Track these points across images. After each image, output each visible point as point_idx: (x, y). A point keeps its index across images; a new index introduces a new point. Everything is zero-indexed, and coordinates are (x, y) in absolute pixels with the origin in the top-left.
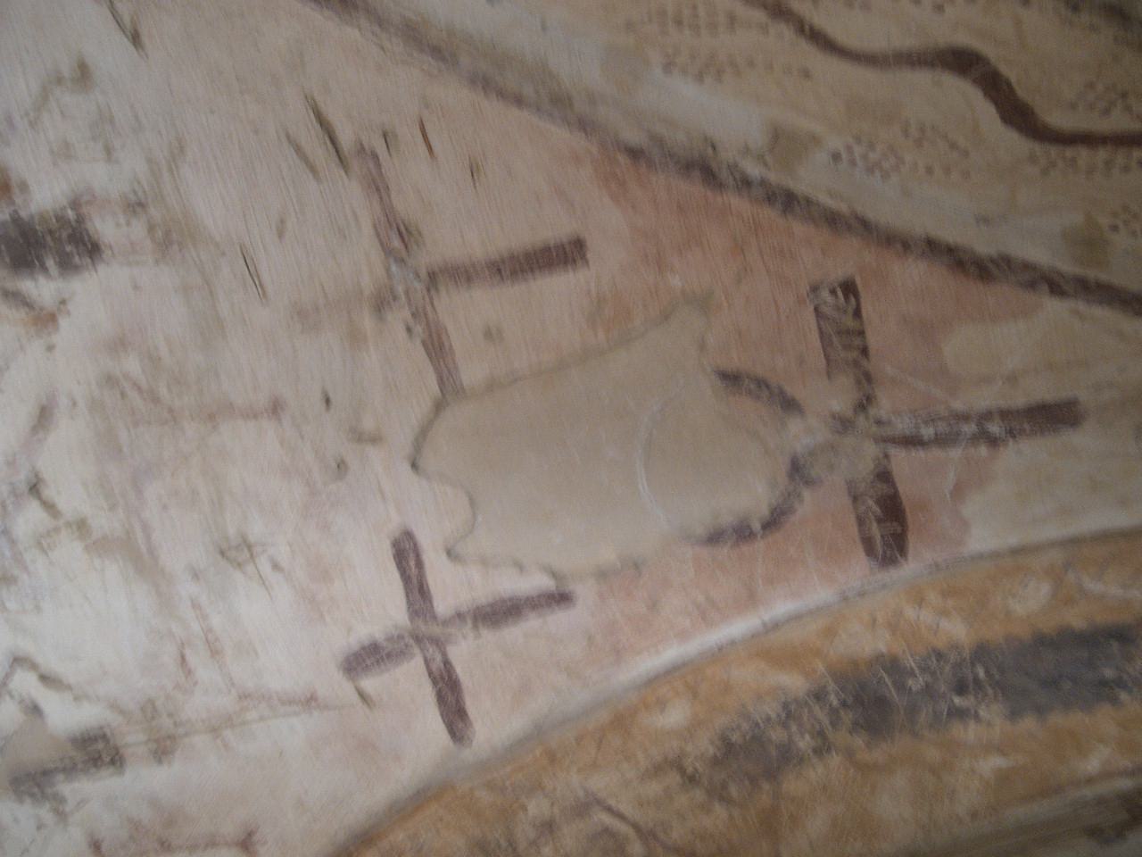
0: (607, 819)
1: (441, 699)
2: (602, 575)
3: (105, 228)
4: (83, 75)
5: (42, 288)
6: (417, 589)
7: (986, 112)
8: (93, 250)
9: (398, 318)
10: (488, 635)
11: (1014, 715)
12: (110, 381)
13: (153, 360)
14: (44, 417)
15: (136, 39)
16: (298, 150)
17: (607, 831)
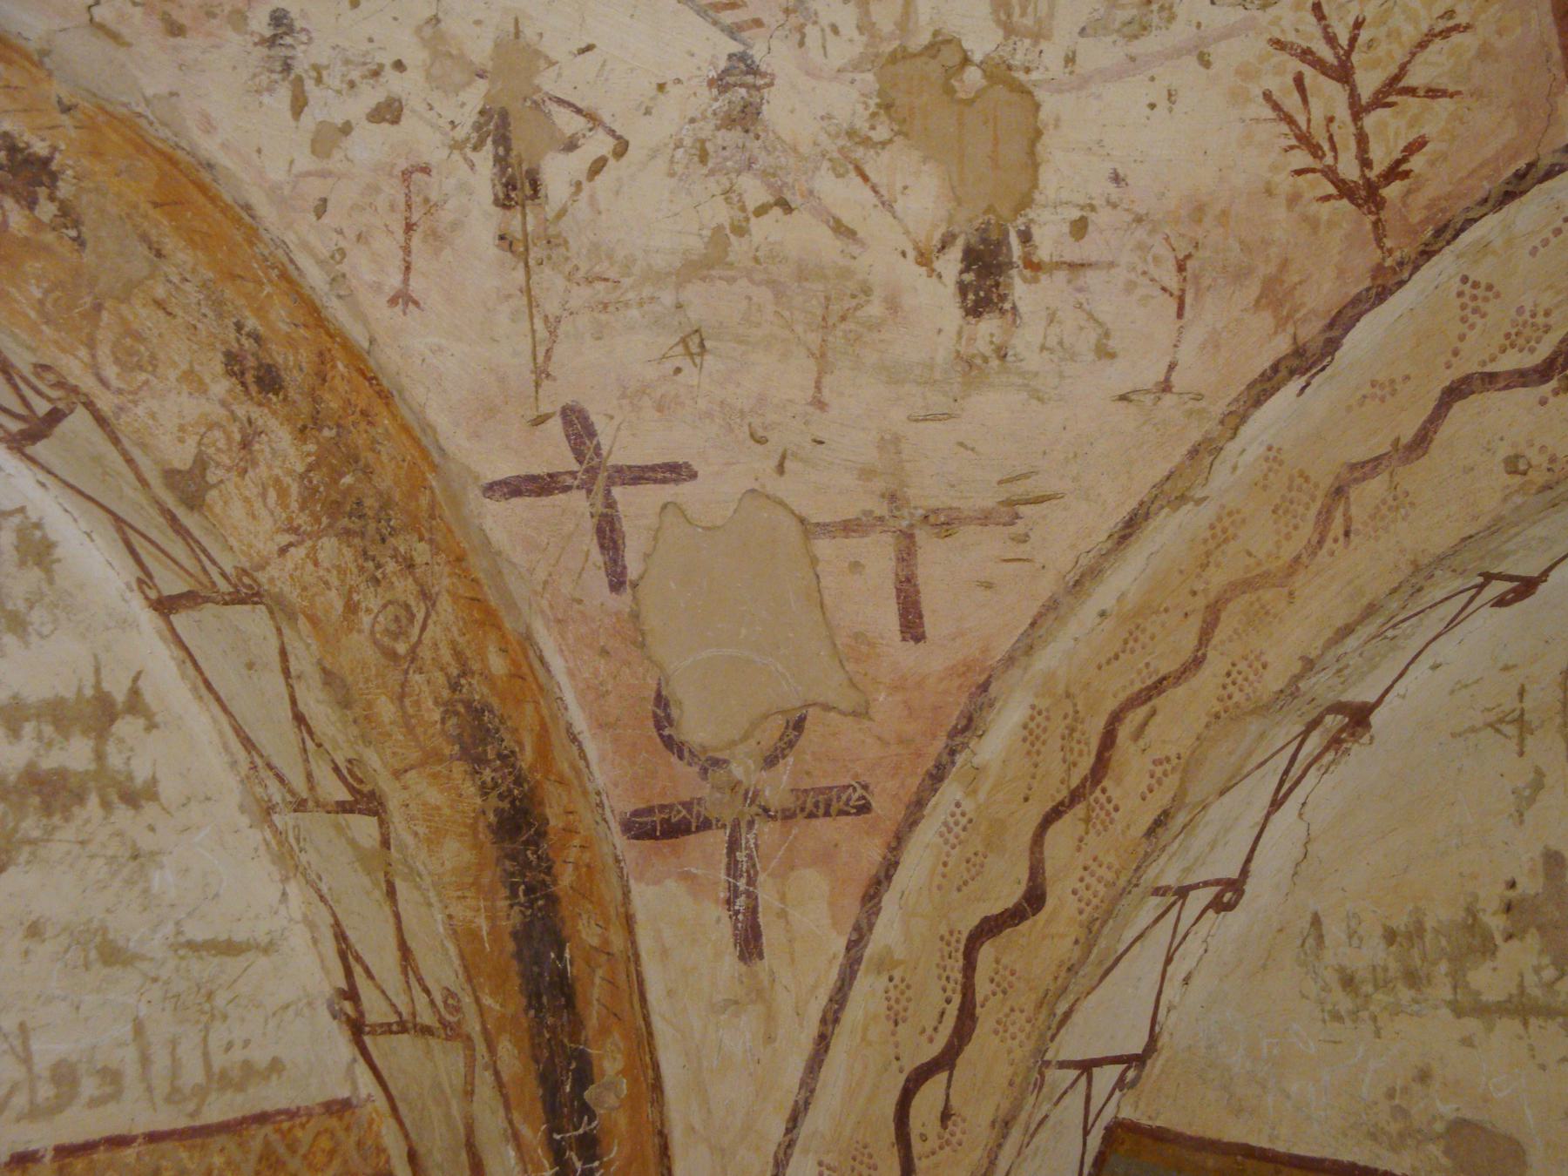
0: (420, 616)
1: (533, 479)
2: (635, 616)
3: (989, 326)
4: (1105, 353)
5: (952, 264)
6: (639, 475)
7: (996, 908)
8: (975, 311)
9: (882, 509)
10: (589, 525)
11: (515, 935)
12: (867, 291)
13: (875, 326)
14: (841, 229)
15: (1123, 398)
16: (1026, 476)
17: (412, 617)
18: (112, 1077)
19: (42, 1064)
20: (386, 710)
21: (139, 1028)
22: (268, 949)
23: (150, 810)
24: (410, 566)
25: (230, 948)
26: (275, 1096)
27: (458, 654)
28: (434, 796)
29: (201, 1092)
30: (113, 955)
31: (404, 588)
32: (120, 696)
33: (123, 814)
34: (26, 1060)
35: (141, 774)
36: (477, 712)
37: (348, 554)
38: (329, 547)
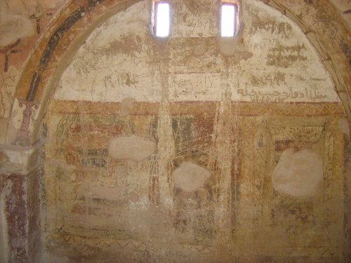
18: (303, 95)
19: (293, 92)
20: (330, 45)
21: (306, 89)
22: (324, 80)
23: (306, 61)
24: (334, 25)
25: (318, 80)
26: (326, 100)
27: (342, 37)
28: (339, 57)
29: (315, 98)
30: (302, 79)
31: (333, 28)
32: (301, 45)
33: (302, 62)
34: (291, 91)
35: (305, 55)
36: (345, 45)
37: (323, 24)
38: (320, 23)
